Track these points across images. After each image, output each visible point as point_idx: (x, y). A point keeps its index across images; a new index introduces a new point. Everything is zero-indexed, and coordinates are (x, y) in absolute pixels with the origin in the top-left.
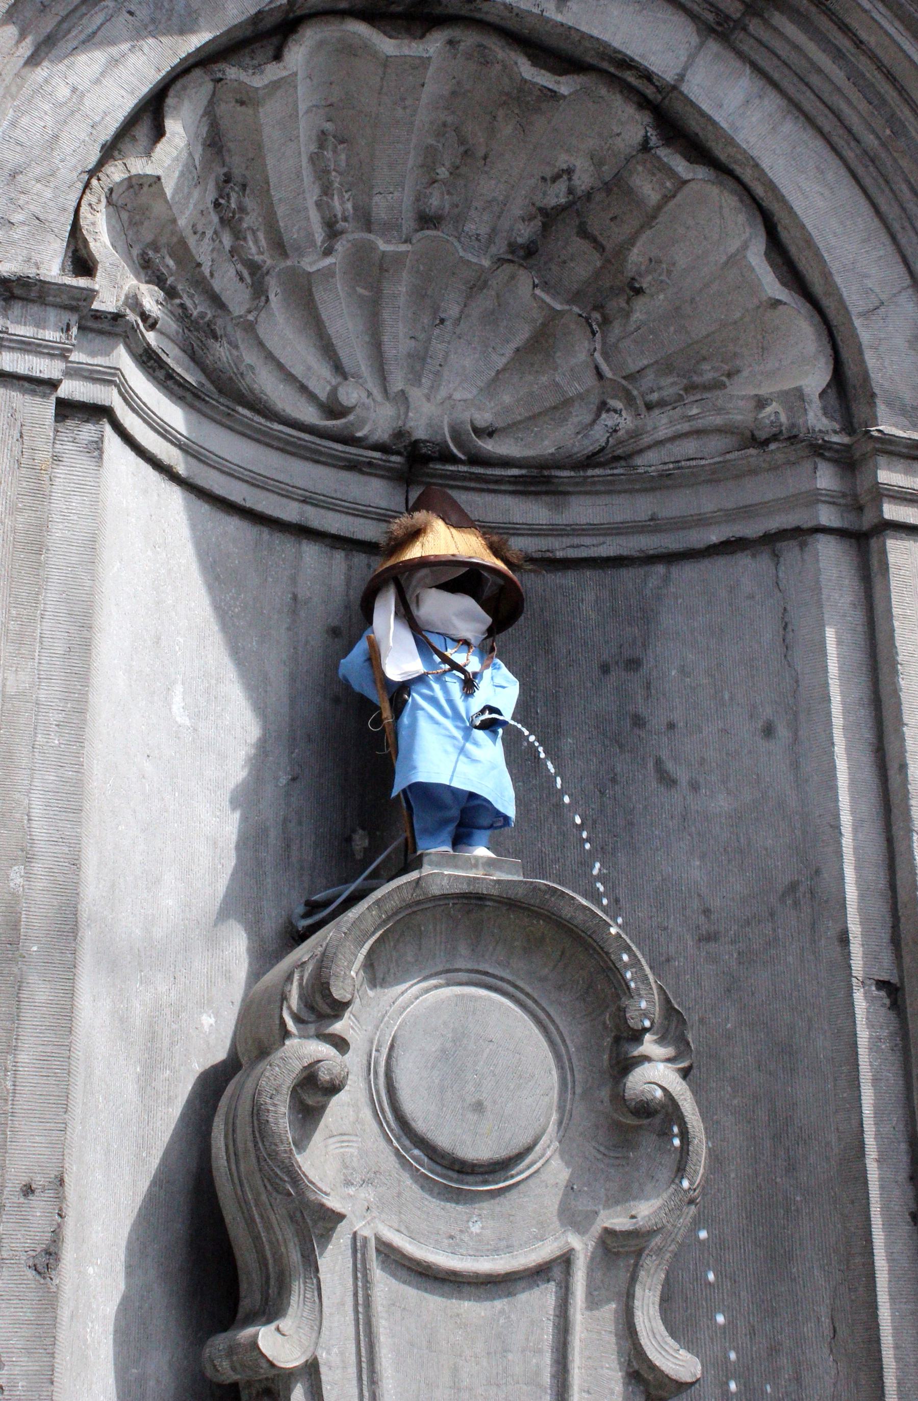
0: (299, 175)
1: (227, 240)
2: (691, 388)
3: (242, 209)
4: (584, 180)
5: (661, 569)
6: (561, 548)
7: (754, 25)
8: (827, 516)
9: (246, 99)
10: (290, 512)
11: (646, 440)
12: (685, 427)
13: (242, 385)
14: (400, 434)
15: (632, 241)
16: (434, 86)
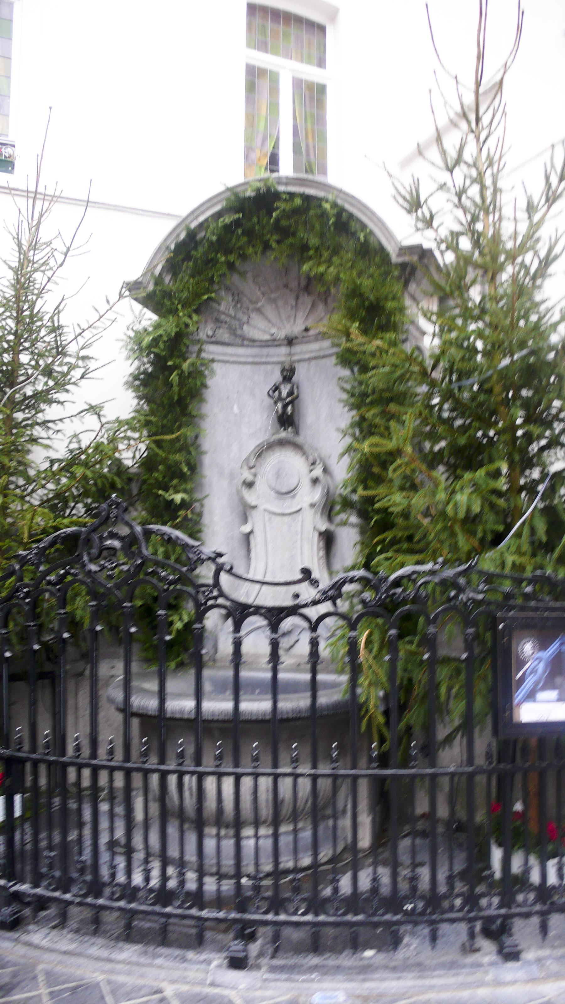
6: (322, 353)
10: (264, 360)
14: (286, 336)
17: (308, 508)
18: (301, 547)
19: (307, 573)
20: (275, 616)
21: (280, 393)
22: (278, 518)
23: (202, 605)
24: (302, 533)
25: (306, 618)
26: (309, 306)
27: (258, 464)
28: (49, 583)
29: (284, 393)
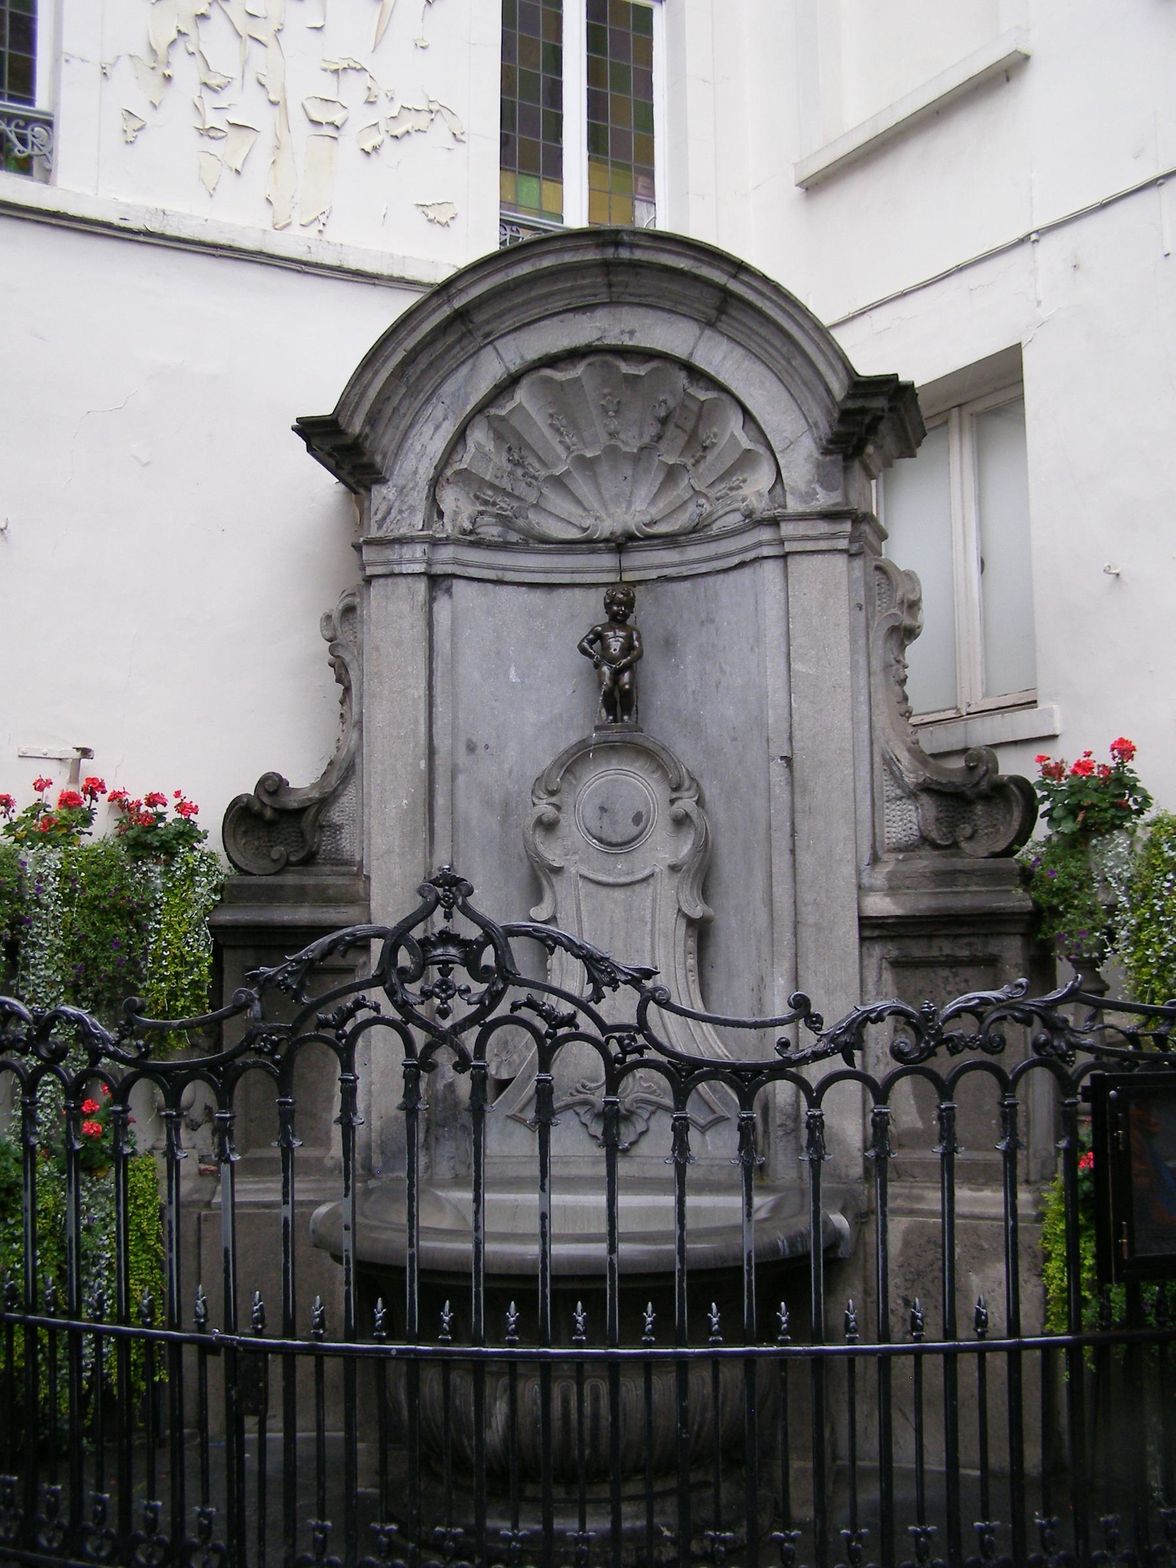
0: (544, 437)
1: (520, 472)
2: (731, 489)
3: (522, 458)
4: (672, 403)
5: (721, 577)
6: (685, 570)
7: (724, 317)
8: (766, 551)
9: (502, 419)
10: (566, 579)
11: (715, 517)
12: (727, 509)
13: (534, 532)
14: (612, 533)
15: (696, 426)
16: (589, 385)
17: (666, 871)
18: (653, 948)
19: (801, 1005)
20: (746, 1079)
21: (606, 647)
22: (604, 892)
23: (617, 1060)
24: (653, 922)
25: (801, 1083)
26: (661, 477)
27: (565, 786)
28: (324, 1024)
29: (615, 646)
